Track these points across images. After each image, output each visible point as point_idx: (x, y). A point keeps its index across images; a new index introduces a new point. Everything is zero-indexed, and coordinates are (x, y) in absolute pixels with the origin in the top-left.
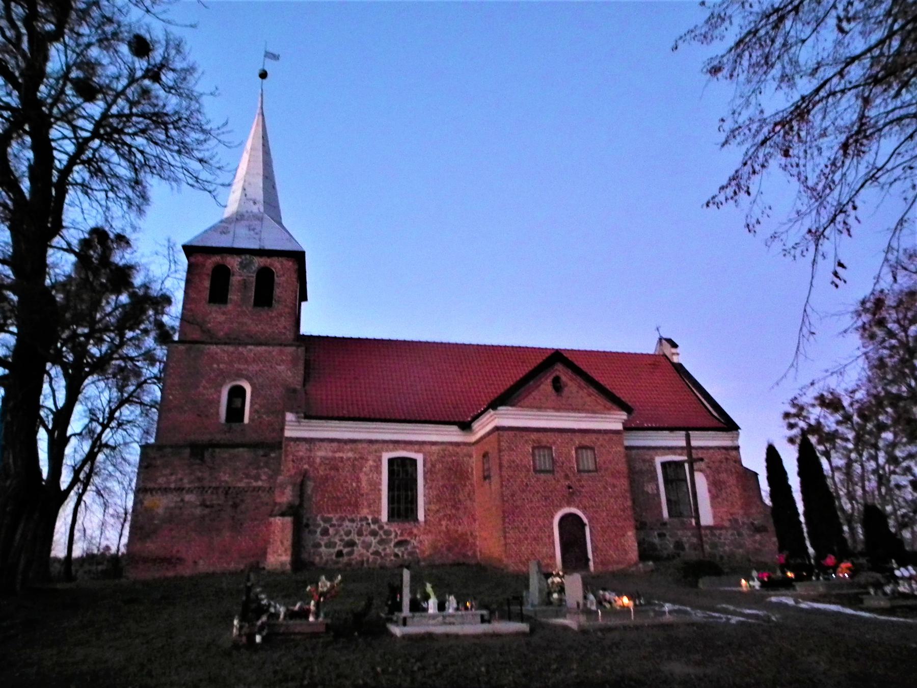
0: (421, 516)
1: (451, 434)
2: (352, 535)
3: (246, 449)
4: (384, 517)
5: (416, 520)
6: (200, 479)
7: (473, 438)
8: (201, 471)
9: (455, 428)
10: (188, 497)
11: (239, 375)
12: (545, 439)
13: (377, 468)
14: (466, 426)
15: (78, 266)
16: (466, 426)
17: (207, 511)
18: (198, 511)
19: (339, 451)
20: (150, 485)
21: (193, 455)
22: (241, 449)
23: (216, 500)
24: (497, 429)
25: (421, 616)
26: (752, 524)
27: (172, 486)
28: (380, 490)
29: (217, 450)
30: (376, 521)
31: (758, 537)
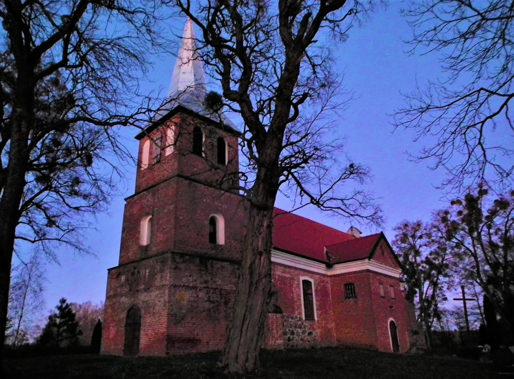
0: (316, 318)
1: (320, 269)
2: (308, 332)
3: (228, 263)
4: (304, 318)
5: (314, 320)
6: (206, 282)
7: (330, 273)
8: (206, 276)
9: (324, 266)
10: (201, 294)
11: (217, 211)
12: (383, 279)
13: (299, 284)
14: (329, 266)
15: (212, 45)
16: (329, 266)
17: (211, 306)
18: (207, 305)
19: (284, 272)
20: (178, 283)
21: (201, 262)
22: (226, 263)
23: (215, 297)
24: (368, 271)
25: (23, 286)
26: (412, 330)
27: (191, 285)
28: (300, 300)
29: (214, 262)
30: (301, 319)
31: (415, 337)
